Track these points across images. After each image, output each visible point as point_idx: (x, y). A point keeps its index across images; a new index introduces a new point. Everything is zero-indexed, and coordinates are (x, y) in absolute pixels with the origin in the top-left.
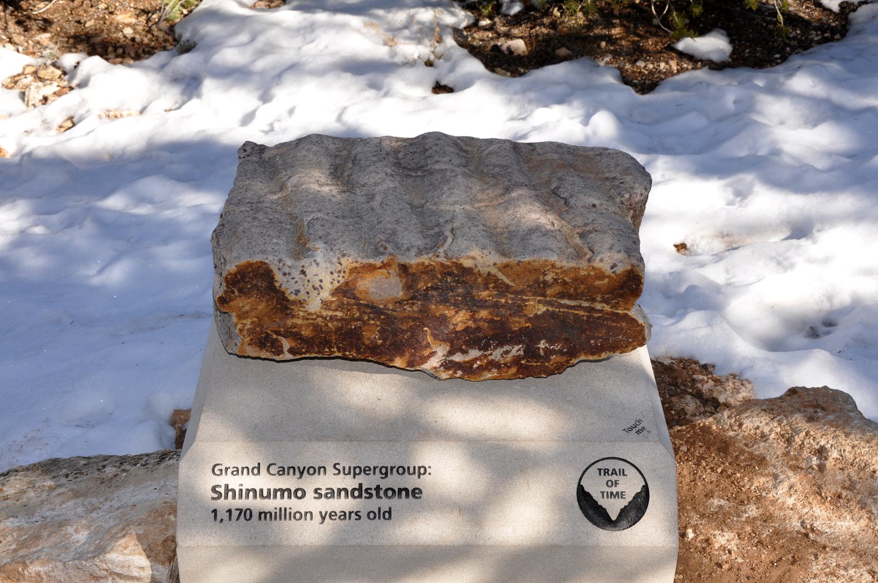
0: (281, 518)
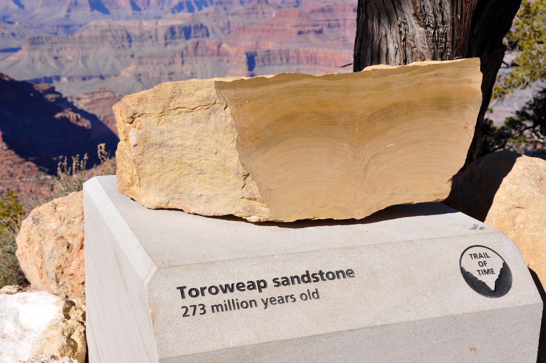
0: (230, 309)
